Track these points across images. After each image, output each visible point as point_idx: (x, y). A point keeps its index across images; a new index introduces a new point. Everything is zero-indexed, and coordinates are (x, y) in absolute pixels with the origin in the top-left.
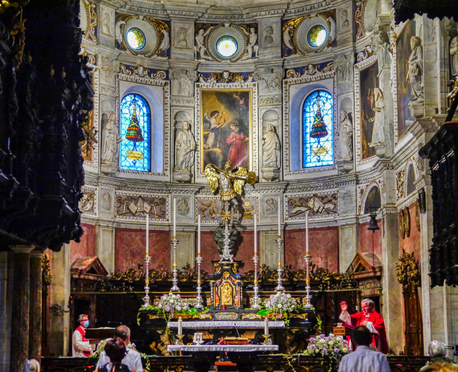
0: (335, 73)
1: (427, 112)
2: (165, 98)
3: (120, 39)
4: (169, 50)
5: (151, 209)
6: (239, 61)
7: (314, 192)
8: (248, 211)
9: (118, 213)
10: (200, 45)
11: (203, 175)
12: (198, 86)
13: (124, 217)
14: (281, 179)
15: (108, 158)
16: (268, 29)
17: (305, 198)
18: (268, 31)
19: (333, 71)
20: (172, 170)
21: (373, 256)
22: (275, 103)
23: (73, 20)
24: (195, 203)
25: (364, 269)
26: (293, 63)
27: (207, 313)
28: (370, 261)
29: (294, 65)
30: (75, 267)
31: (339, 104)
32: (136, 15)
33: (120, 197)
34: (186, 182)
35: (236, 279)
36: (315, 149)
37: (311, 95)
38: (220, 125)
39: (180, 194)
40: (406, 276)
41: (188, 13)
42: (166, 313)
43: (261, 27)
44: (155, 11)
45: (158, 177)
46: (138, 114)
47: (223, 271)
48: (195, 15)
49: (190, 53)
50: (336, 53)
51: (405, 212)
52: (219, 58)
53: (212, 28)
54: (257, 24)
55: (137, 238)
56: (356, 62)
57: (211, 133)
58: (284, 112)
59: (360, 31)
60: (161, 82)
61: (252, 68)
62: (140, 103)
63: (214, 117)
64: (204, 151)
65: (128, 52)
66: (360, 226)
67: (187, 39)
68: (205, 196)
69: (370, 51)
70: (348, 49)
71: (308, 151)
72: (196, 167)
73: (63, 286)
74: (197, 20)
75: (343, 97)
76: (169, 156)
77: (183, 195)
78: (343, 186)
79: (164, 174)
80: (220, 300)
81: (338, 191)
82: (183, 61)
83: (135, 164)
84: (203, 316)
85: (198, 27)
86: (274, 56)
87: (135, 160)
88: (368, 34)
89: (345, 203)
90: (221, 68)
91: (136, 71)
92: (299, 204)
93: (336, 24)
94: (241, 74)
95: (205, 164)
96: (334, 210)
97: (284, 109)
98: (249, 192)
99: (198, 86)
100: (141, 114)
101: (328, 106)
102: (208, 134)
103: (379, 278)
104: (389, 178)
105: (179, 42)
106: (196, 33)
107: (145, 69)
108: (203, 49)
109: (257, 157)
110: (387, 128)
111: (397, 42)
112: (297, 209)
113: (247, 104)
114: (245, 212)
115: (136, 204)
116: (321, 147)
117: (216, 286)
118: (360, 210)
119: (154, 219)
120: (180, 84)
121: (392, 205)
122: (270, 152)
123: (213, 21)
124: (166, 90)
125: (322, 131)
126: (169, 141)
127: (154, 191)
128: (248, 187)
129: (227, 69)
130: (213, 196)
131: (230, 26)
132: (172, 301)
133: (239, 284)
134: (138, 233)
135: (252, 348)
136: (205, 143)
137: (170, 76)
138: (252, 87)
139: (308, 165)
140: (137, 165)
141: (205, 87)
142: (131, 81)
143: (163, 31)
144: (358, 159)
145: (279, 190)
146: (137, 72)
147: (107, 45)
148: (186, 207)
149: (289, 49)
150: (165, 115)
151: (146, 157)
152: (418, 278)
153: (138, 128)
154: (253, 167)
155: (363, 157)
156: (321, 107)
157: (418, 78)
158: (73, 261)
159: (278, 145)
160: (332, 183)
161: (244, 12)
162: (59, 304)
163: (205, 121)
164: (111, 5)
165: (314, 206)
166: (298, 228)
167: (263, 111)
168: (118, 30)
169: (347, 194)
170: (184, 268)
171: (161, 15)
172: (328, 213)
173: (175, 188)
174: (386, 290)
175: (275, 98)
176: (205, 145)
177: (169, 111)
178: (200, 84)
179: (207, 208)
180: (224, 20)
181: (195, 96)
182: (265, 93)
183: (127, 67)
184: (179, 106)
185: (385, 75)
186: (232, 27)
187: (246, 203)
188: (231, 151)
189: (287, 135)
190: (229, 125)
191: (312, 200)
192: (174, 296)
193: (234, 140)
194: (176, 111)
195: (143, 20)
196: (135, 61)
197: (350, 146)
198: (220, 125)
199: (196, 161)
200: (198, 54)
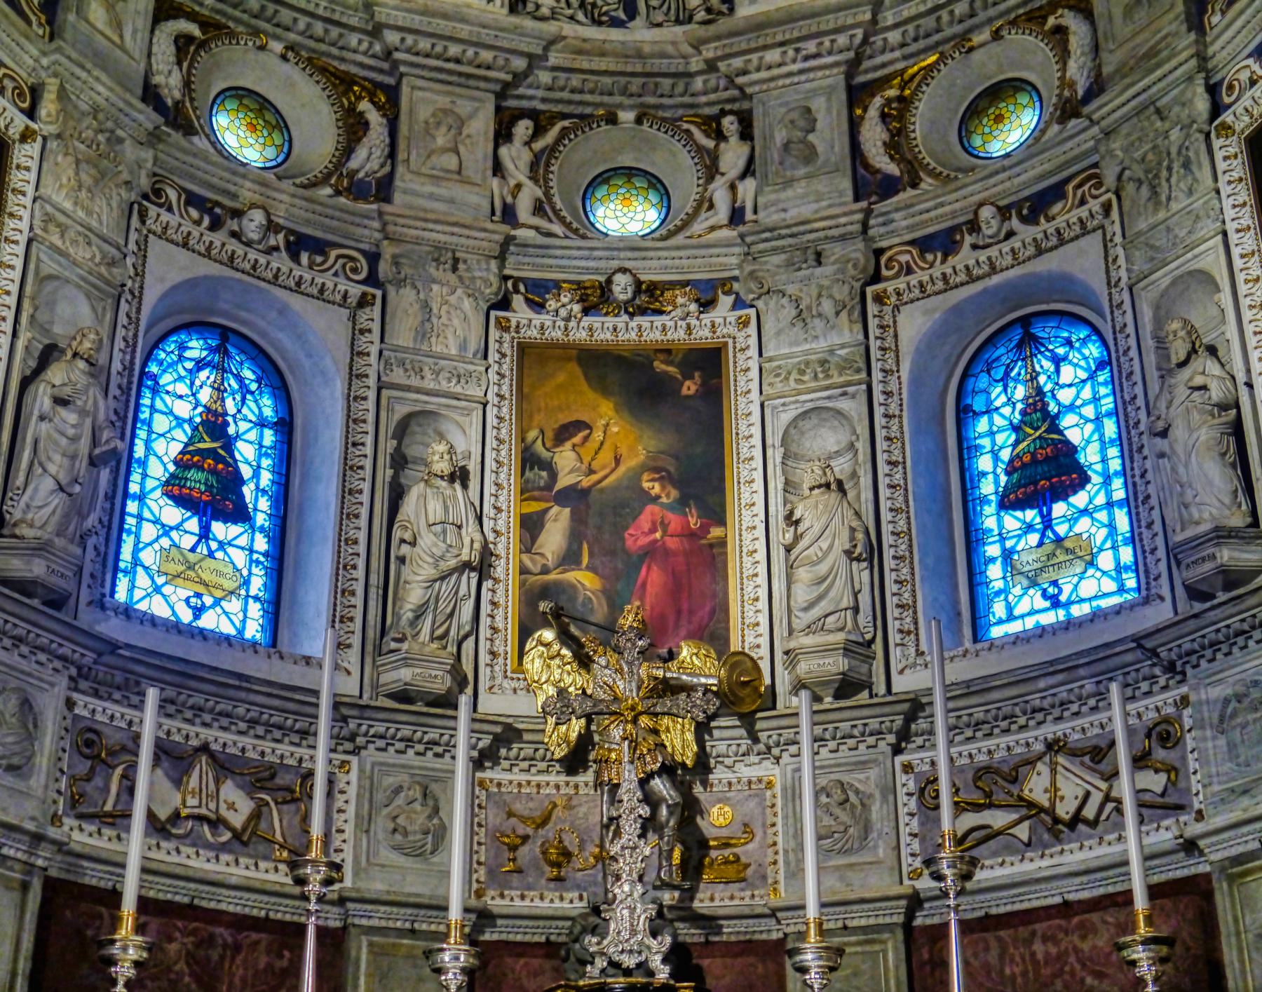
0: (1107, 208)
2: (356, 353)
5: (256, 816)
6: (679, 239)
7: (1050, 730)
8: (727, 845)
9: (74, 803)
11: (514, 684)
12: (504, 327)
13: (107, 832)
14: (881, 689)
16: (795, 115)
17: (1006, 769)
18: (792, 122)
20: (369, 648)
22: (837, 379)
26: (904, 223)
29: (911, 228)
31: (1147, 314)
33: (90, 730)
38: (594, 478)
39: (401, 760)
41: (470, 52)
43: (765, 114)
44: (335, 32)
45: (300, 669)
48: (501, 62)
50: (1104, 123)
53: (566, 123)
55: (173, 947)
56: (1217, 109)
57: (556, 509)
58: (879, 411)
60: (341, 288)
61: (729, 261)
63: (568, 445)
64: (522, 584)
67: (462, 149)
68: (524, 777)
71: (995, 571)
72: (484, 646)
76: (359, 588)
77: (418, 762)
78: (1216, 665)
81: (1184, 701)
83: (198, 611)
86: (824, 203)
87: (198, 595)
89: (1232, 746)
90: (603, 264)
91: (233, 225)
95: (525, 633)
96: (1167, 800)
97: (878, 397)
98: (728, 761)
102: (546, 511)
105: (429, 156)
106: (503, 135)
107: (271, 227)
108: (530, 192)
109: (763, 604)
114: (713, 854)
115: (178, 783)
116: (1059, 540)
119: (271, 865)
120: (426, 306)
122: (823, 568)
123: (570, 102)
125: (1059, 475)
126: (363, 522)
127: (277, 734)
129: (628, 264)
130: (563, 778)
131: (639, 121)
134: (180, 924)
137: (384, 268)
138: (732, 330)
139: (996, 632)
141: (534, 333)
142: (207, 254)
143: (364, 106)
145: (871, 740)
146: (236, 228)
148: (430, 817)
151: (256, 598)
153: (227, 464)
156: (1042, 379)
159: (860, 536)
160: (1146, 671)
163: (529, 460)
166: (981, 913)
167: (786, 417)
169: (1239, 698)
173: (380, 728)
175: (834, 360)
176: (525, 558)
177: (370, 404)
179: (530, 831)
180: (618, 99)
181: (491, 360)
183: (192, 200)
184: (418, 391)
186: (645, 126)
187: (715, 810)
188: (644, 585)
189: (900, 503)
190: (636, 475)
191: (1040, 766)
193: (658, 535)
194: (401, 410)
195: (284, 57)
196: (232, 188)
197: (1233, 466)
198: (594, 478)
199: (484, 621)
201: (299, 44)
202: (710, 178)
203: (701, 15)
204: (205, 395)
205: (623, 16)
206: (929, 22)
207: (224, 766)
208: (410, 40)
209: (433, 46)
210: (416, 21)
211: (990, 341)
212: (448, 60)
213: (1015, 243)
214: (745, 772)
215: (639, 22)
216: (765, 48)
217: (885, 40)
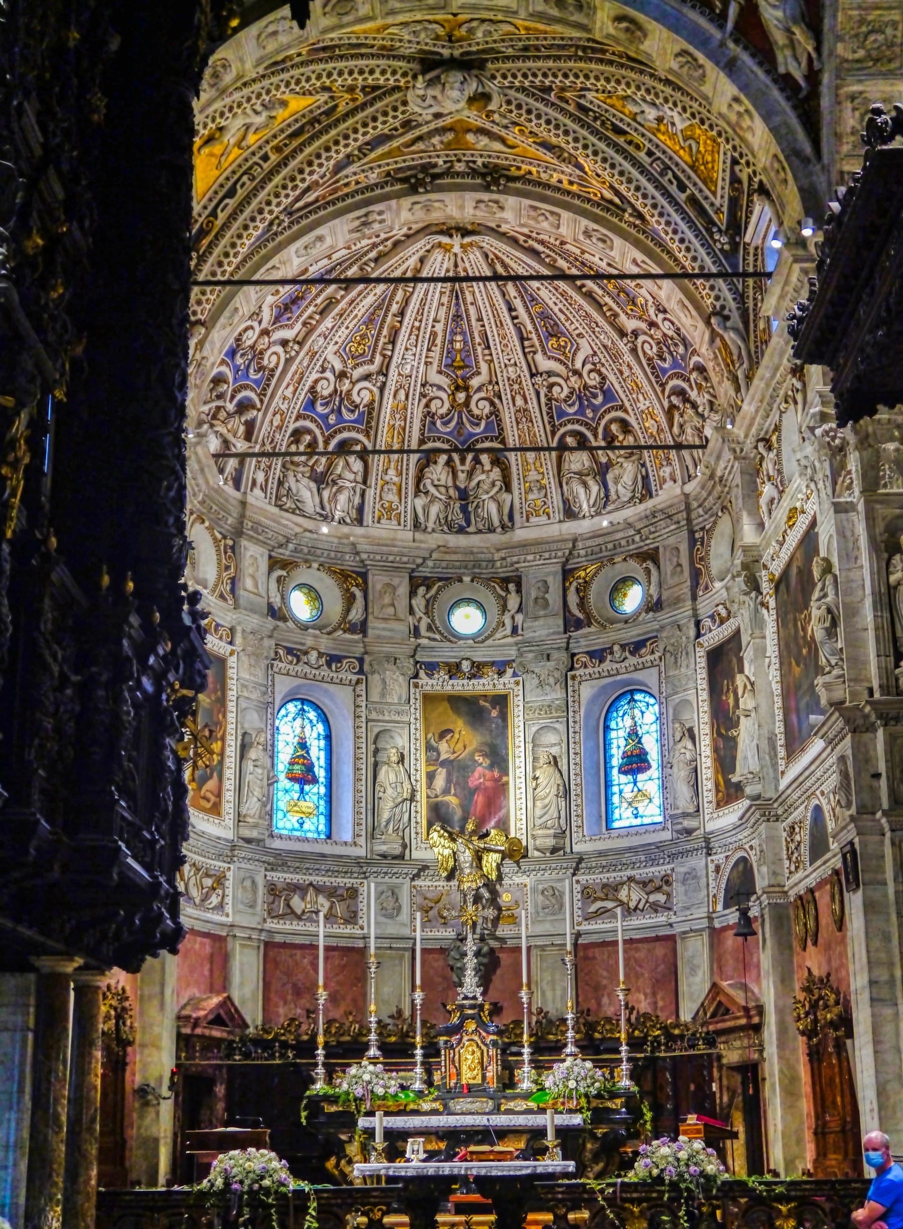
1: (854, 695)
2: (357, 706)
3: (276, 601)
4: (364, 623)
5: (331, 908)
6: (490, 642)
7: (629, 873)
10: (419, 614)
12: (416, 686)
14: (568, 850)
15: (252, 812)
19: (657, 655)
21: (745, 988)
23: (171, 520)
24: (412, 896)
25: (727, 1011)
27: (435, 1100)
28: (739, 997)
30: (185, 1013)
31: (671, 712)
32: (306, 561)
34: (395, 858)
35: (488, 1033)
36: (628, 795)
37: (618, 698)
40: (815, 1021)
42: (355, 1100)
46: (307, 734)
47: (464, 1018)
49: (401, 628)
51: (807, 900)
52: (452, 636)
54: (520, 577)
55: (306, 961)
56: (698, 635)
59: (703, 580)
61: (513, 653)
62: (312, 715)
65: (290, 624)
66: (716, 934)
69: (724, 613)
70: (684, 613)
71: (616, 799)
73: (158, 1048)
74: (413, 570)
75: (677, 698)
79: (355, 844)
80: (459, 1074)
82: (390, 641)
83: (302, 824)
84: (426, 1106)
85: (416, 583)
88: (718, 585)
91: (304, 658)
92: (602, 895)
94: (493, 664)
95: (430, 825)
97: (571, 724)
99: (416, 686)
100: (315, 735)
101: (650, 716)
103: (758, 1028)
104: (771, 838)
106: (413, 593)
107: (321, 655)
108: (425, 621)
110: (764, 745)
111: (777, 588)
112: (599, 904)
113: (504, 716)
115: (303, 899)
117: (452, 1047)
118: (715, 903)
120: (384, 681)
121: (777, 888)
124: (358, 692)
128: (509, 867)
129: (468, 654)
132: (366, 1077)
133: (495, 1043)
135: (522, 1168)
136: (429, 785)
137: (366, 667)
139: (616, 825)
140: (306, 826)
143: (354, 589)
144: (708, 808)
147: (253, 610)
149: (578, 619)
150: (357, 737)
152: (845, 1023)
154: (518, 828)
155: (718, 806)
157: (831, 632)
158: (184, 1001)
161: (497, 556)
162: (152, 1084)
163: (429, 748)
165: (630, 899)
167: (534, 729)
168: (273, 585)
170: (391, 1017)
171: (350, 562)
172: (656, 911)
174: (771, 1050)
178: (420, 682)
182: (537, 698)
183: (290, 651)
185: (756, 650)
190: (472, 755)
192: (371, 1068)
194: (376, 730)
200: (417, 629)
202: (503, 613)
204: (298, 730)
207: (318, 890)
211: (618, 698)
213: (626, 663)
214: (517, 880)
215: (472, 529)
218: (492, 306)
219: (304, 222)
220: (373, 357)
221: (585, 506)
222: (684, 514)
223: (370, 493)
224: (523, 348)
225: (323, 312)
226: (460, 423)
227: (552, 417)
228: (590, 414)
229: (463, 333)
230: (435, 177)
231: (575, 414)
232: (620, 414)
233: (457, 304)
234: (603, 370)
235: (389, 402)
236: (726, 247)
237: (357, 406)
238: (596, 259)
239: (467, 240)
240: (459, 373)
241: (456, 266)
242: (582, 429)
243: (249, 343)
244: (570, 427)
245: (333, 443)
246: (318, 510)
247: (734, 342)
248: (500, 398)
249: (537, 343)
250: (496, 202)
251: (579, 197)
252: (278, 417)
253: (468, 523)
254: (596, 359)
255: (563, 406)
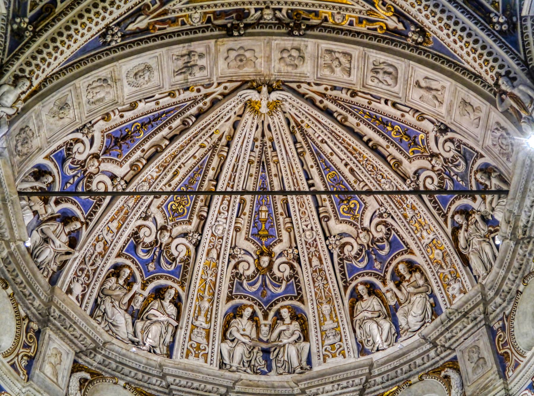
41: (203, 386)
44: (146, 377)
93: (460, 374)
164: (67, 336)
195: (125, 387)
201: (131, 382)
203: (298, 370)
205: (266, 370)
206: (392, 374)
208: (177, 380)
209: (187, 383)
210: (181, 373)
212: (193, 389)
215: (273, 373)
216: (325, 384)
217: (375, 380)
218: (293, 174)
219: (135, 48)
220: (191, 218)
221: (378, 339)
222: (481, 307)
223: (181, 333)
224: (319, 214)
225: (149, 160)
226: (264, 285)
227: (344, 275)
228: (377, 265)
229: (268, 205)
230: (247, 26)
231: (365, 268)
232: (406, 256)
233: (264, 178)
234: (389, 220)
235: (202, 260)
236: (505, 27)
237: (174, 259)
238: (382, 106)
239: (275, 96)
240: (264, 240)
241: (263, 135)
242: (373, 279)
243: (81, 158)
244: (360, 279)
245: (151, 286)
246: (131, 337)
247: (524, 93)
248: (299, 261)
249: (330, 209)
250: (298, 50)
251: (367, 35)
252: (101, 244)
253: (270, 369)
254: (383, 209)
255: (354, 263)
